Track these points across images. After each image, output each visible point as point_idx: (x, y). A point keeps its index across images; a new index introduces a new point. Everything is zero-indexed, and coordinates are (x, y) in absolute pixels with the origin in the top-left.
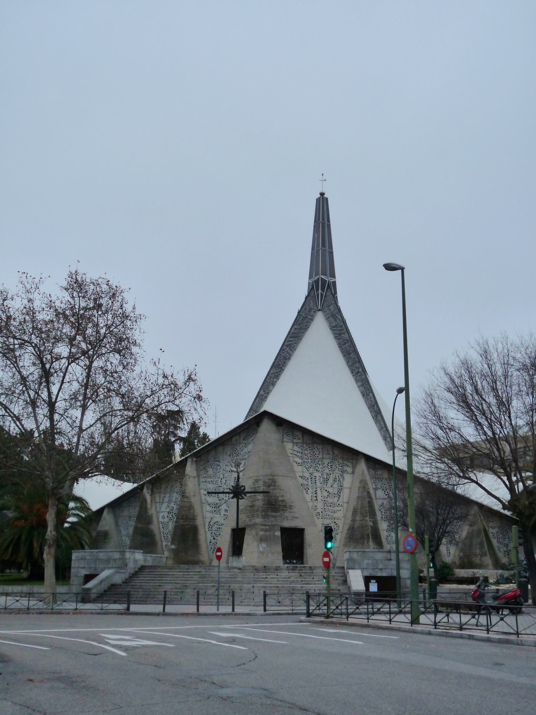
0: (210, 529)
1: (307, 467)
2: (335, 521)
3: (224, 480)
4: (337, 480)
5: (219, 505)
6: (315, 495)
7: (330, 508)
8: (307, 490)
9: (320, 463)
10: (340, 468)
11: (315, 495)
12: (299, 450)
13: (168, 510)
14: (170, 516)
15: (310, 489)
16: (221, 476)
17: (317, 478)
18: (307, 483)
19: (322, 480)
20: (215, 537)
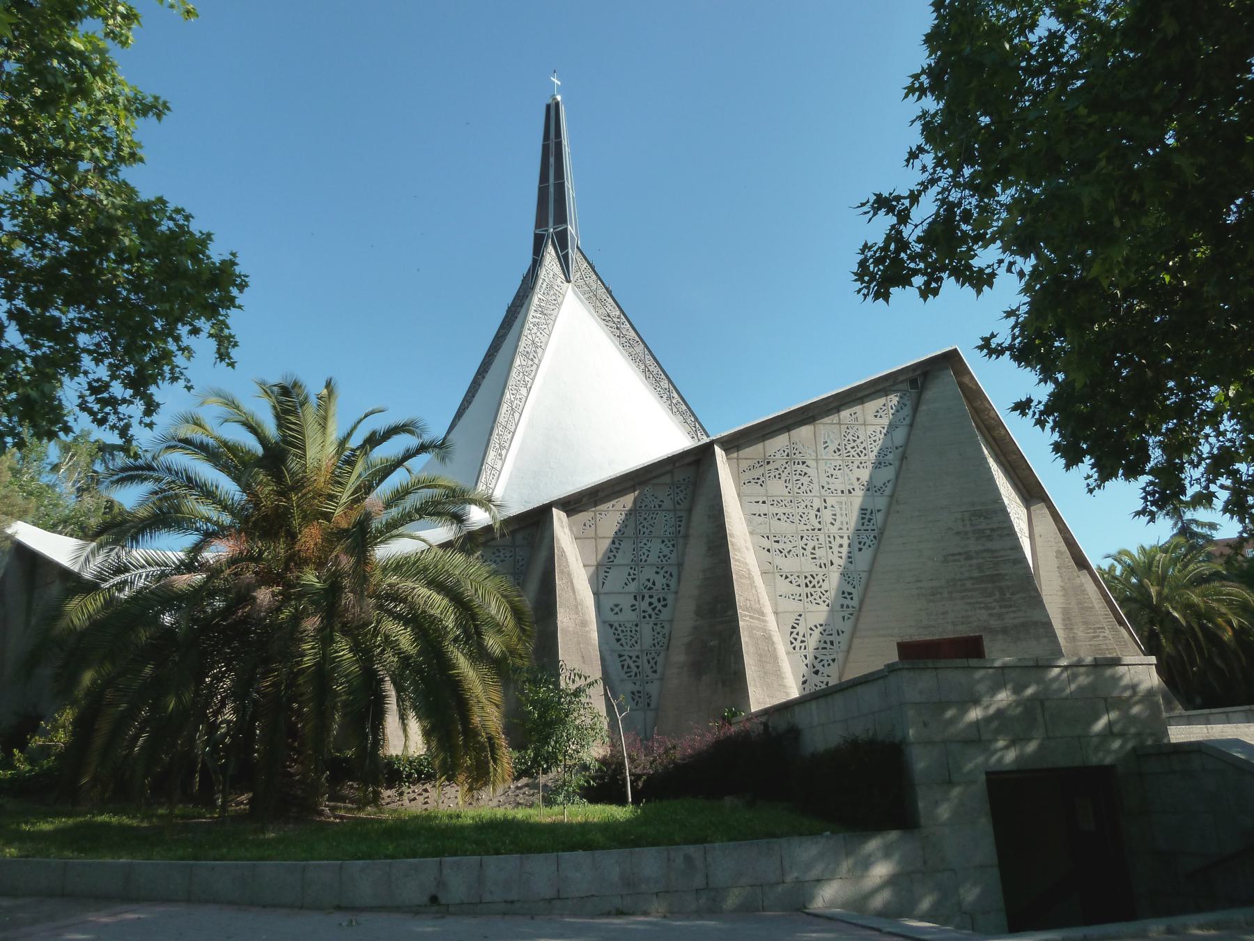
0: (797, 644)
3: (827, 515)
5: (820, 578)
13: (633, 587)
14: (644, 605)
16: (817, 503)
20: (819, 666)
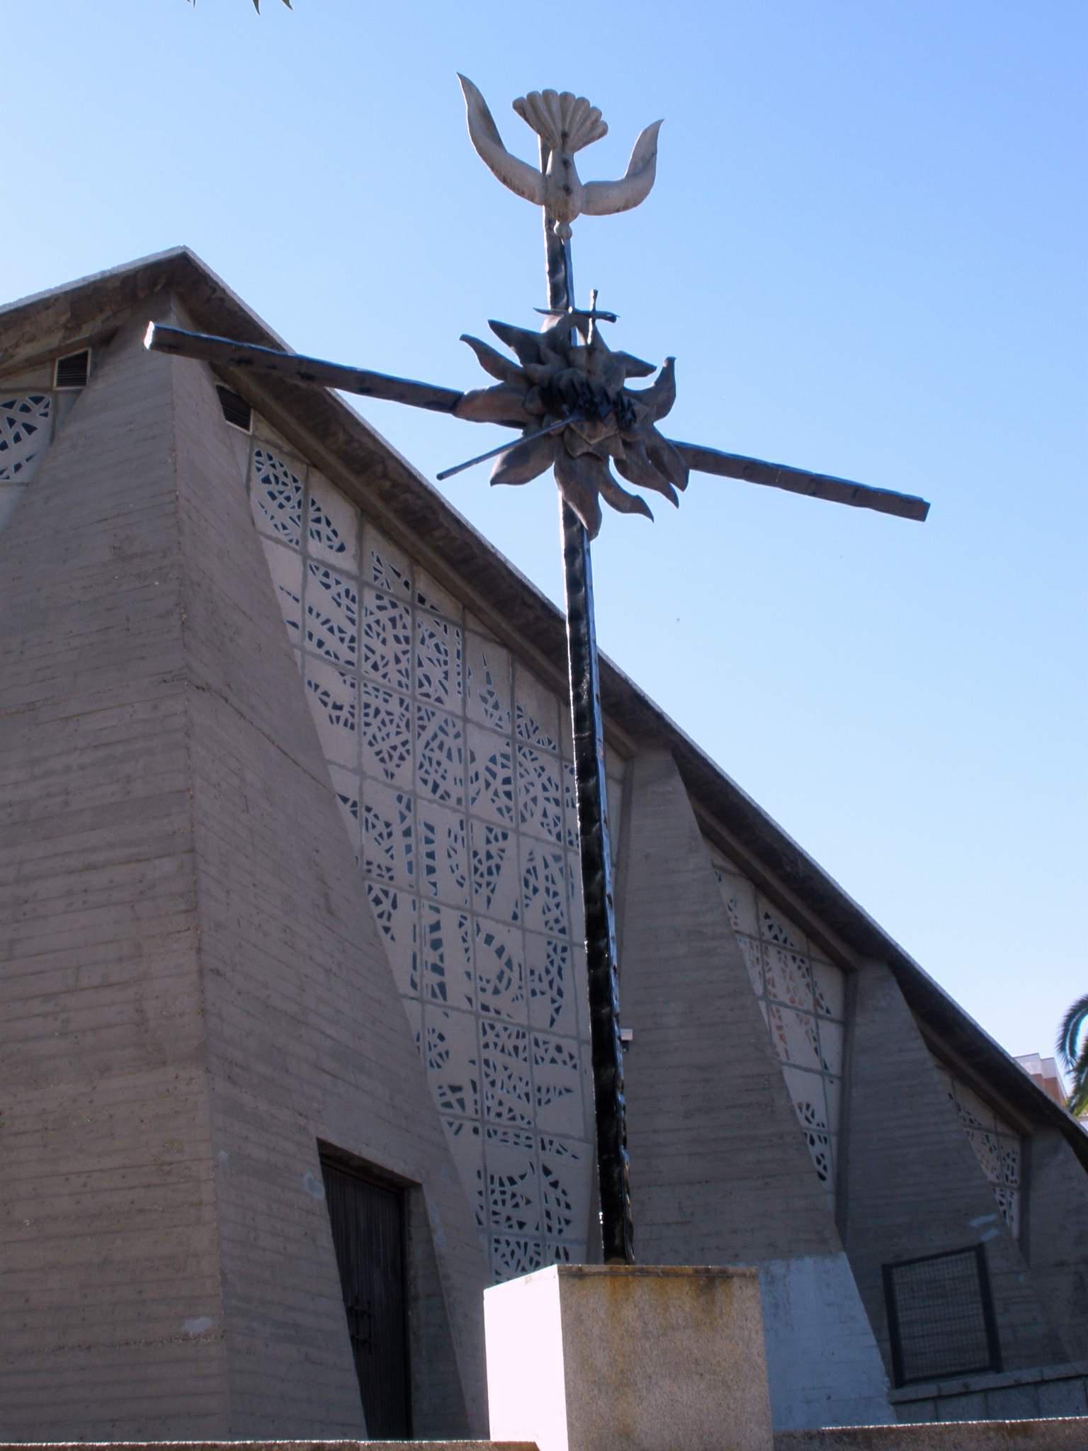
1: (384, 746)
2: (549, 1158)
4: (541, 884)
6: (431, 956)
7: (512, 1062)
8: (386, 905)
9: (450, 742)
10: (553, 810)
11: (431, 956)
12: (339, 617)
15: (404, 900)
17: (442, 843)
18: (385, 861)
19: (462, 858)
